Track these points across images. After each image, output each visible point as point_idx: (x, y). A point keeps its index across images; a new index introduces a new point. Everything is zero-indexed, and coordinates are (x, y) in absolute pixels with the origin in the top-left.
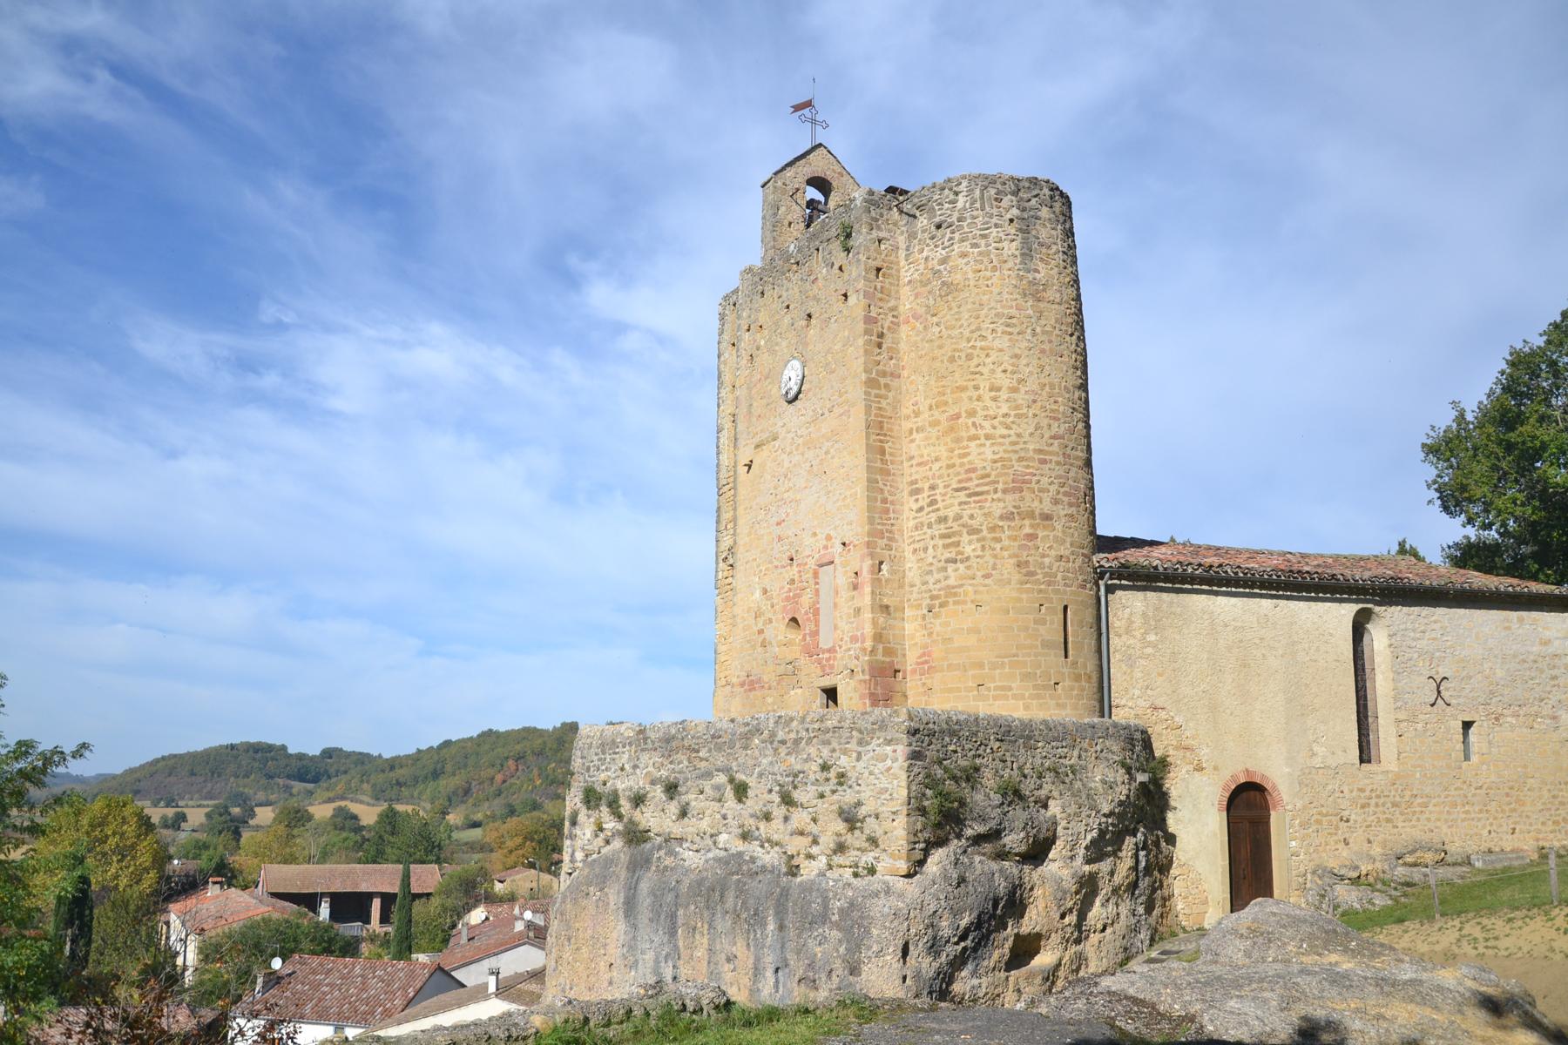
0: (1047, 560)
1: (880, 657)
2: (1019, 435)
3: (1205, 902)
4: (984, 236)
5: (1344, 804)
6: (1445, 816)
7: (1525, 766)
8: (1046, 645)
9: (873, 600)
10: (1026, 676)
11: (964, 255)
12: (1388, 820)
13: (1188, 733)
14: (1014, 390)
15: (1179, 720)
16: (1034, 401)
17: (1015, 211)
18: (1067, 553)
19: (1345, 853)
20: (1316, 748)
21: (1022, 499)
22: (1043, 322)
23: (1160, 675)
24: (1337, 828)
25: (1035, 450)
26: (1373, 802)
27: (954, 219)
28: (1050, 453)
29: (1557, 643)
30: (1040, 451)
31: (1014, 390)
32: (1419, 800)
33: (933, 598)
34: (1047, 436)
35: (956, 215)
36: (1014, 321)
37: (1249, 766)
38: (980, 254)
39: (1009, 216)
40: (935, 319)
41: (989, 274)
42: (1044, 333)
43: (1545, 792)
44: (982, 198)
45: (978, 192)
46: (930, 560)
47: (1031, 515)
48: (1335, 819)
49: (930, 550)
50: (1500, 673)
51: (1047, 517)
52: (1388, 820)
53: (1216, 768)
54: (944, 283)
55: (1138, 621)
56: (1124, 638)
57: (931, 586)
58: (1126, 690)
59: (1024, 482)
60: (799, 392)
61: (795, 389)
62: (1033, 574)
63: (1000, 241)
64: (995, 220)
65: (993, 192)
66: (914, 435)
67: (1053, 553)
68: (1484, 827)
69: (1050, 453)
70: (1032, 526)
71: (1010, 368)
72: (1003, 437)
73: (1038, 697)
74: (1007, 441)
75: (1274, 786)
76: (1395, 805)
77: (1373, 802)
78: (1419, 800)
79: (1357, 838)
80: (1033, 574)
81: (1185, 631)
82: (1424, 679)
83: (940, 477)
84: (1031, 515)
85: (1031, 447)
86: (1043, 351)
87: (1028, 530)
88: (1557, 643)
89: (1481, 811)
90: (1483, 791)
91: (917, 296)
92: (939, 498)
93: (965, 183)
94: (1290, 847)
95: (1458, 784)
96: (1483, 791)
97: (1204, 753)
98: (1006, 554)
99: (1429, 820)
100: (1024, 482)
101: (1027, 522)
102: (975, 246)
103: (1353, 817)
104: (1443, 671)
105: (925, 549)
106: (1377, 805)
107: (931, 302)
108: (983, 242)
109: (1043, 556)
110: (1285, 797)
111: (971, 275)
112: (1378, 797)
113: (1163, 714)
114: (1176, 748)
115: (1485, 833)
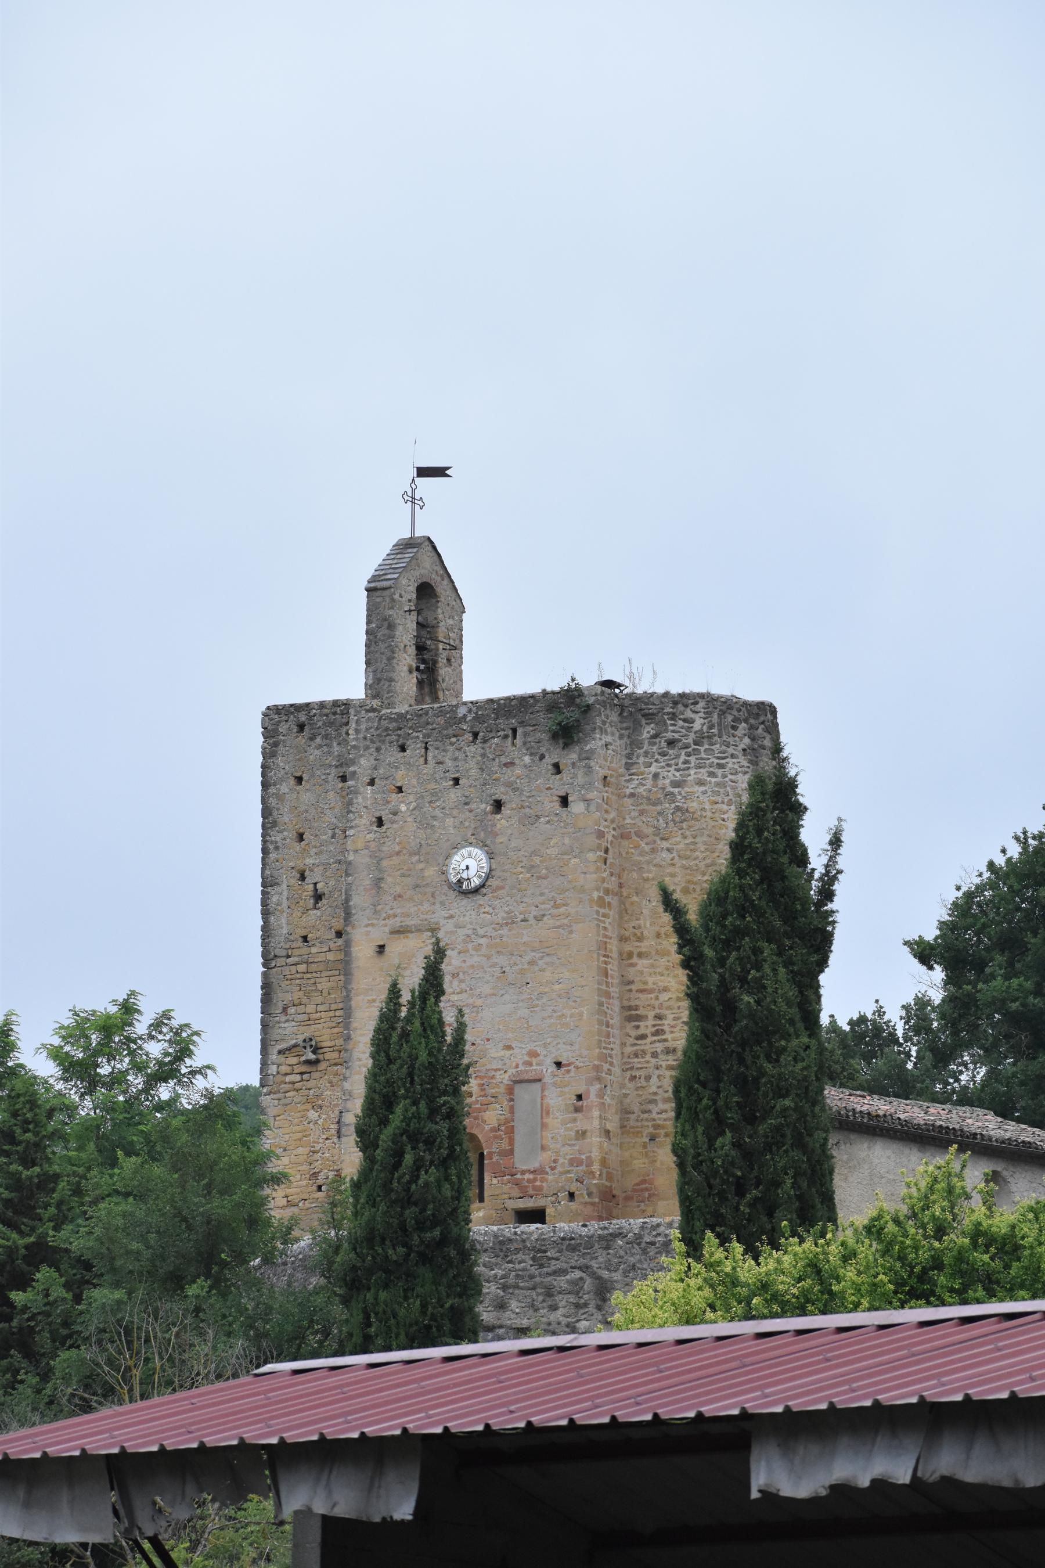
1: (604, 1181)
4: (721, 766)
9: (600, 1124)
11: (701, 783)
17: (747, 740)
27: (690, 740)
33: (656, 1127)
35: (692, 736)
38: (718, 784)
40: (665, 844)
41: (725, 807)
44: (720, 724)
45: (715, 716)
46: (654, 1089)
49: (654, 1080)
54: (678, 809)
57: (654, 1115)
60: (483, 886)
61: (476, 882)
63: (736, 773)
64: (731, 750)
65: (730, 718)
66: (635, 960)
81: (851, 1179)
83: (669, 1008)
91: (642, 812)
92: (666, 1028)
93: (702, 704)
102: (712, 774)
105: (648, 1078)
107: (662, 824)
108: (719, 772)
111: (707, 806)
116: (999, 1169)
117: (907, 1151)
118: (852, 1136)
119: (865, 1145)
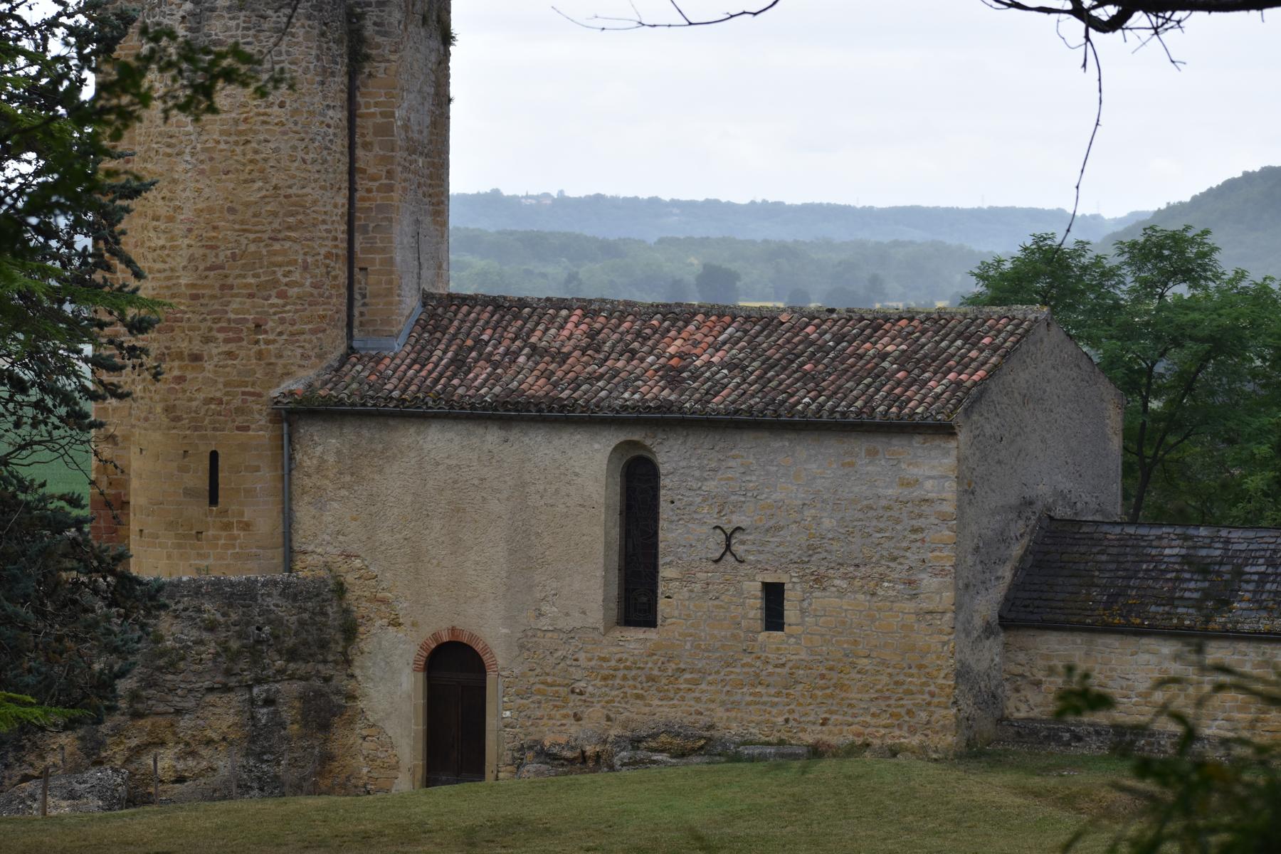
0: (194, 404)
2: (172, 270)
3: (396, 767)
5: (578, 674)
6: (724, 697)
7: (856, 643)
8: (188, 492)
10: (171, 525)
12: (638, 697)
13: (384, 585)
14: (171, 219)
15: (374, 569)
16: (190, 230)
18: (218, 395)
19: (573, 729)
20: (545, 608)
21: (173, 339)
22: (204, 138)
23: (355, 520)
24: (566, 701)
25: (187, 286)
26: (620, 674)
28: (204, 287)
29: (929, 484)
30: (193, 286)
31: (171, 219)
32: (688, 676)
34: (201, 267)
36: (173, 141)
37: (455, 623)
39: (181, 13)
42: (204, 150)
43: (885, 679)
47: (180, 356)
48: (564, 691)
50: (827, 523)
51: (196, 358)
52: (638, 697)
53: (414, 624)
55: (331, 459)
56: (315, 478)
58: (315, 535)
59: (176, 320)
62: (178, 419)
67: (201, 396)
68: (780, 714)
69: (204, 287)
70: (180, 368)
71: (168, 195)
72: (159, 271)
73: (179, 546)
74: (163, 275)
75: (486, 647)
76: (651, 679)
77: (620, 674)
78: (688, 676)
79: (595, 713)
80: (178, 419)
82: (705, 529)
84: (180, 356)
85: (183, 281)
86: (202, 172)
87: (176, 373)
88: (929, 484)
89: (778, 694)
90: (785, 671)
94: (502, 717)
95: (747, 659)
96: (785, 671)
97: (402, 607)
98: (157, 397)
99: (698, 700)
100: (176, 320)
101: (176, 363)
103: (590, 689)
104: (737, 520)
106: (625, 678)
109: (190, 400)
110: (501, 662)
112: (626, 668)
113: (358, 563)
114: (369, 600)
115: (780, 720)
116: (636, 438)
117: (480, 431)
118: (391, 422)
119: (412, 430)
